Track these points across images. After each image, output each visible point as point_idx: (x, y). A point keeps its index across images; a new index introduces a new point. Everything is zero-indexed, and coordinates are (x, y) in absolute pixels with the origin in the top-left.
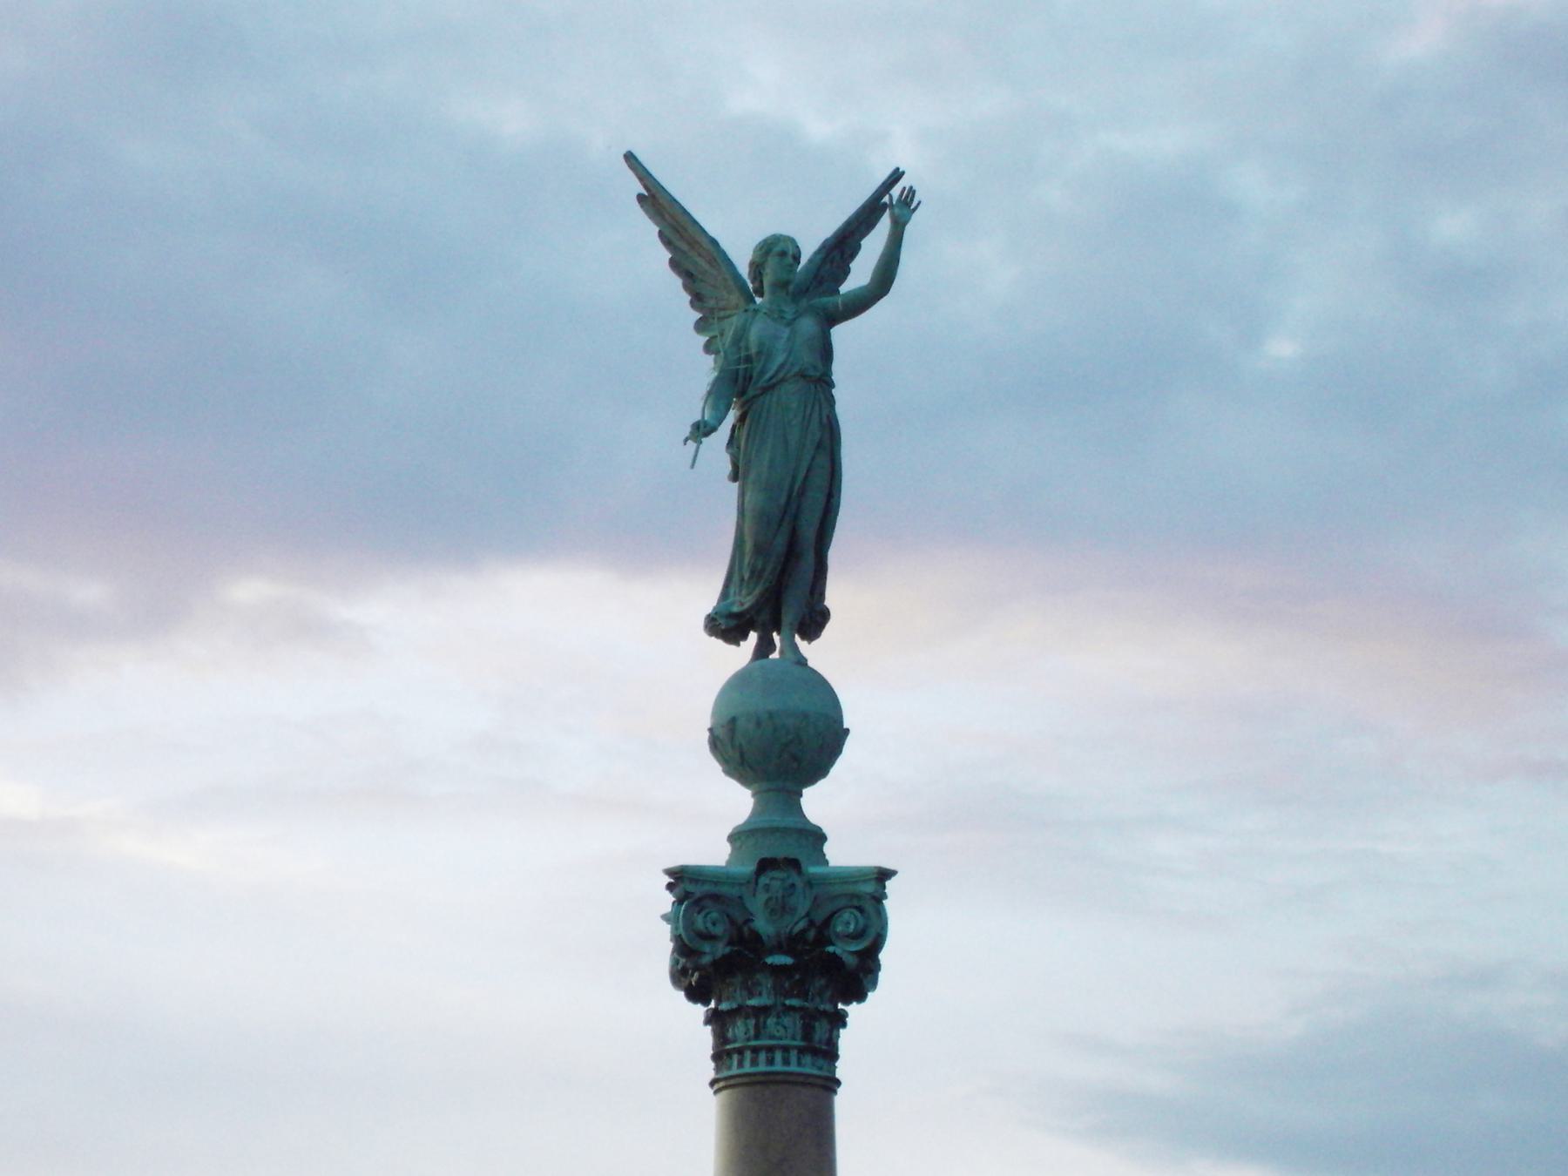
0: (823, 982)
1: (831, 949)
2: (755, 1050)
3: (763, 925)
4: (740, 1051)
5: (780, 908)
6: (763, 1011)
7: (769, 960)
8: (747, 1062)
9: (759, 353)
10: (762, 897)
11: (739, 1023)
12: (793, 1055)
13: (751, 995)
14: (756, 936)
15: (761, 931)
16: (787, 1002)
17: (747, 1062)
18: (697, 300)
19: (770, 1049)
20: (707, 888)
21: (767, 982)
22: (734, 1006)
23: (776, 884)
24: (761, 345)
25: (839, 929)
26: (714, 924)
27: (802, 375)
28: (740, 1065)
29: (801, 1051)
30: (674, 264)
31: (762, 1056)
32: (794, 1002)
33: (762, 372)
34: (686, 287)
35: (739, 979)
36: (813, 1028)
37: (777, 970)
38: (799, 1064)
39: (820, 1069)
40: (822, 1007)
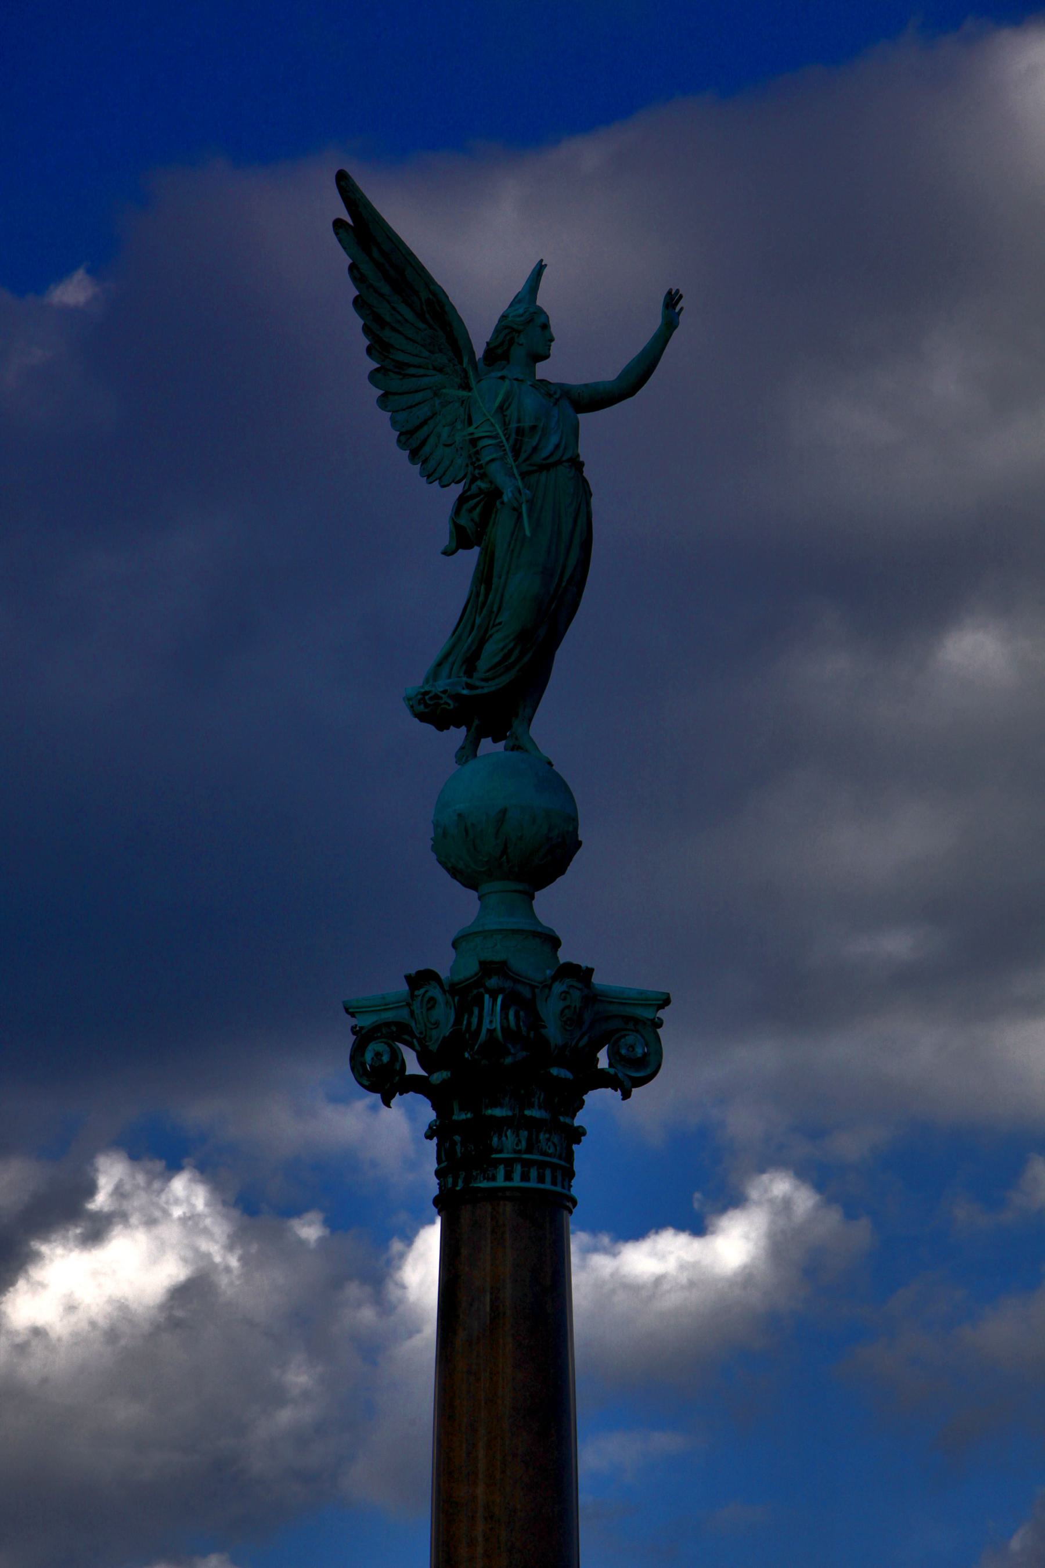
2: (527, 1164)
4: (509, 1163)
9: (534, 428)
18: (378, 347)
19: (542, 1165)
28: (508, 1177)
30: (358, 303)
33: (535, 449)
34: (367, 330)
38: (554, 1183)
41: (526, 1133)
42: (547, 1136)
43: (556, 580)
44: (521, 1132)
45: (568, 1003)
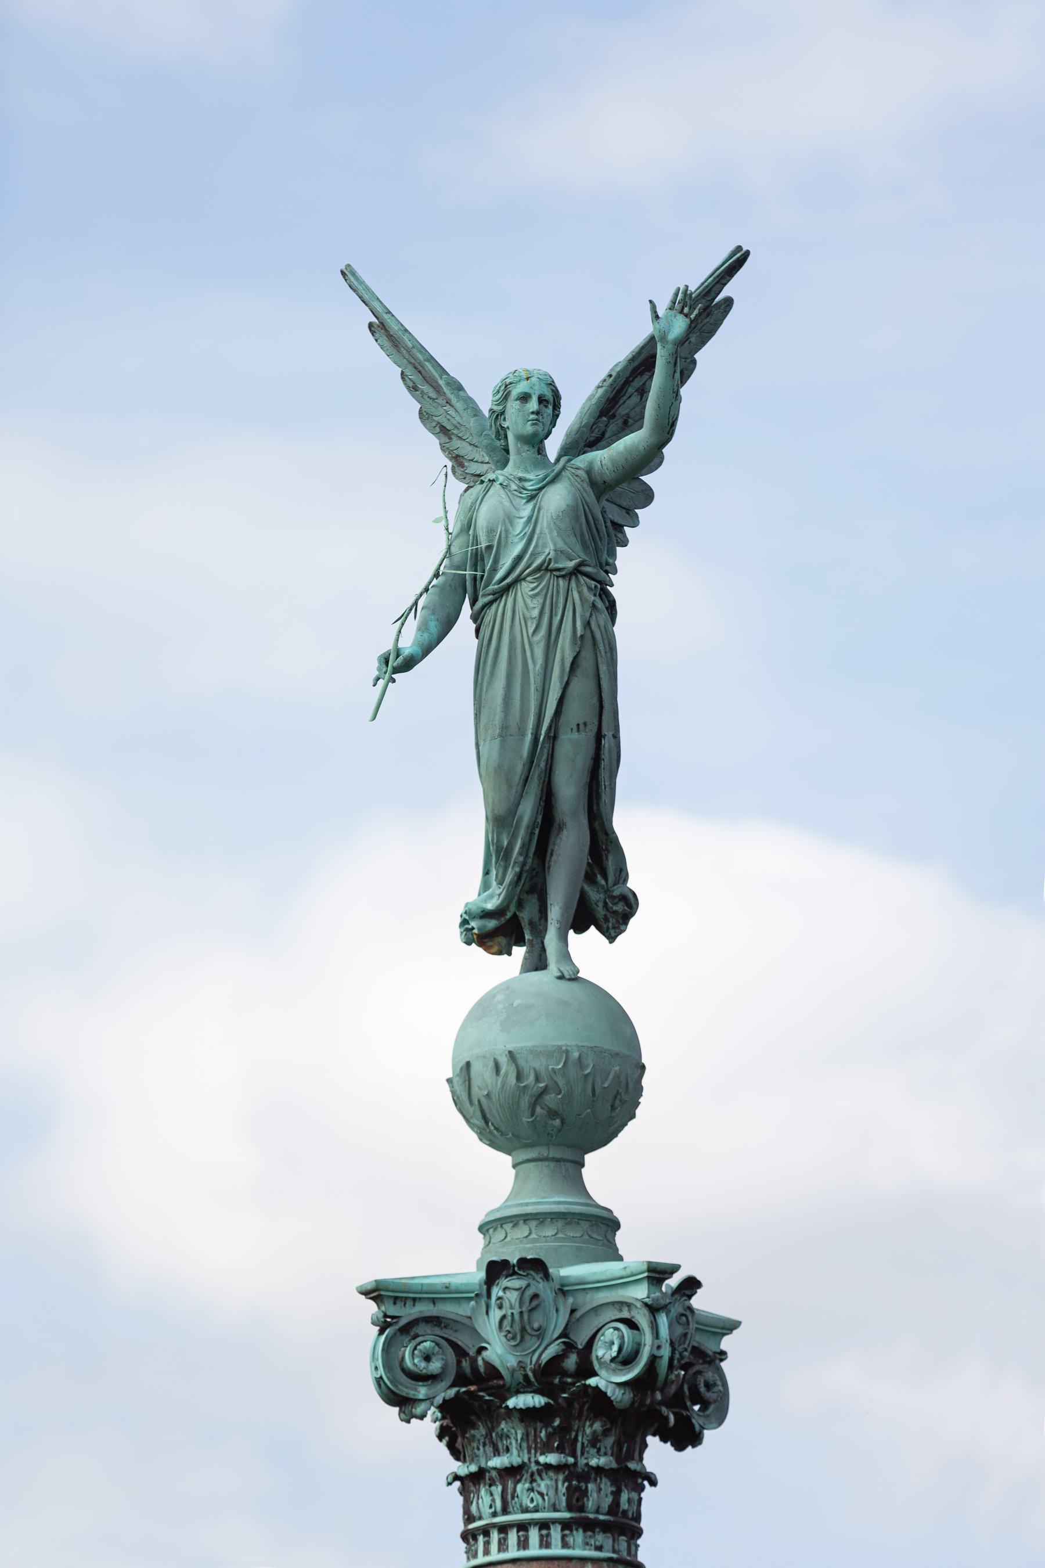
0: (597, 1426)
1: (592, 1381)
2: (503, 1529)
3: (498, 1352)
5: (520, 1332)
6: (513, 1472)
7: (511, 1403)
8: (494, 1546)
9: (489, 548)
10: (496, 1314)
11: (483, 1492)
12: (556, 1533)
13: (497, 1452)
14: (493, 1372)
15: (497, 1364)
16: (542, 1459)
17: (494, 1546)
19: (522, 1527)
20: (423, 1309)
21: (516, 1432)
22: (473, 1468)
23: (513, 1296)
24: (491, 532)
25: (600, 1353)
26: (427, 1358)
27: (545, 568)
28: (487, 1552)
29: (567, 1525)
31: (513, 1536)
32: (552, 1458)
33: (494, 569)
34: (443, 448)
35: (480, 1431)
36: (585, 1493)
37: (527, 1415)
38: (565, 1545)
39: (599, 1548)
40: (594, 1462)
41: (500, 1488)
42: (527, 1485)
43: (529, 738)
44: (493, 1488)
45: (503, 1312)
